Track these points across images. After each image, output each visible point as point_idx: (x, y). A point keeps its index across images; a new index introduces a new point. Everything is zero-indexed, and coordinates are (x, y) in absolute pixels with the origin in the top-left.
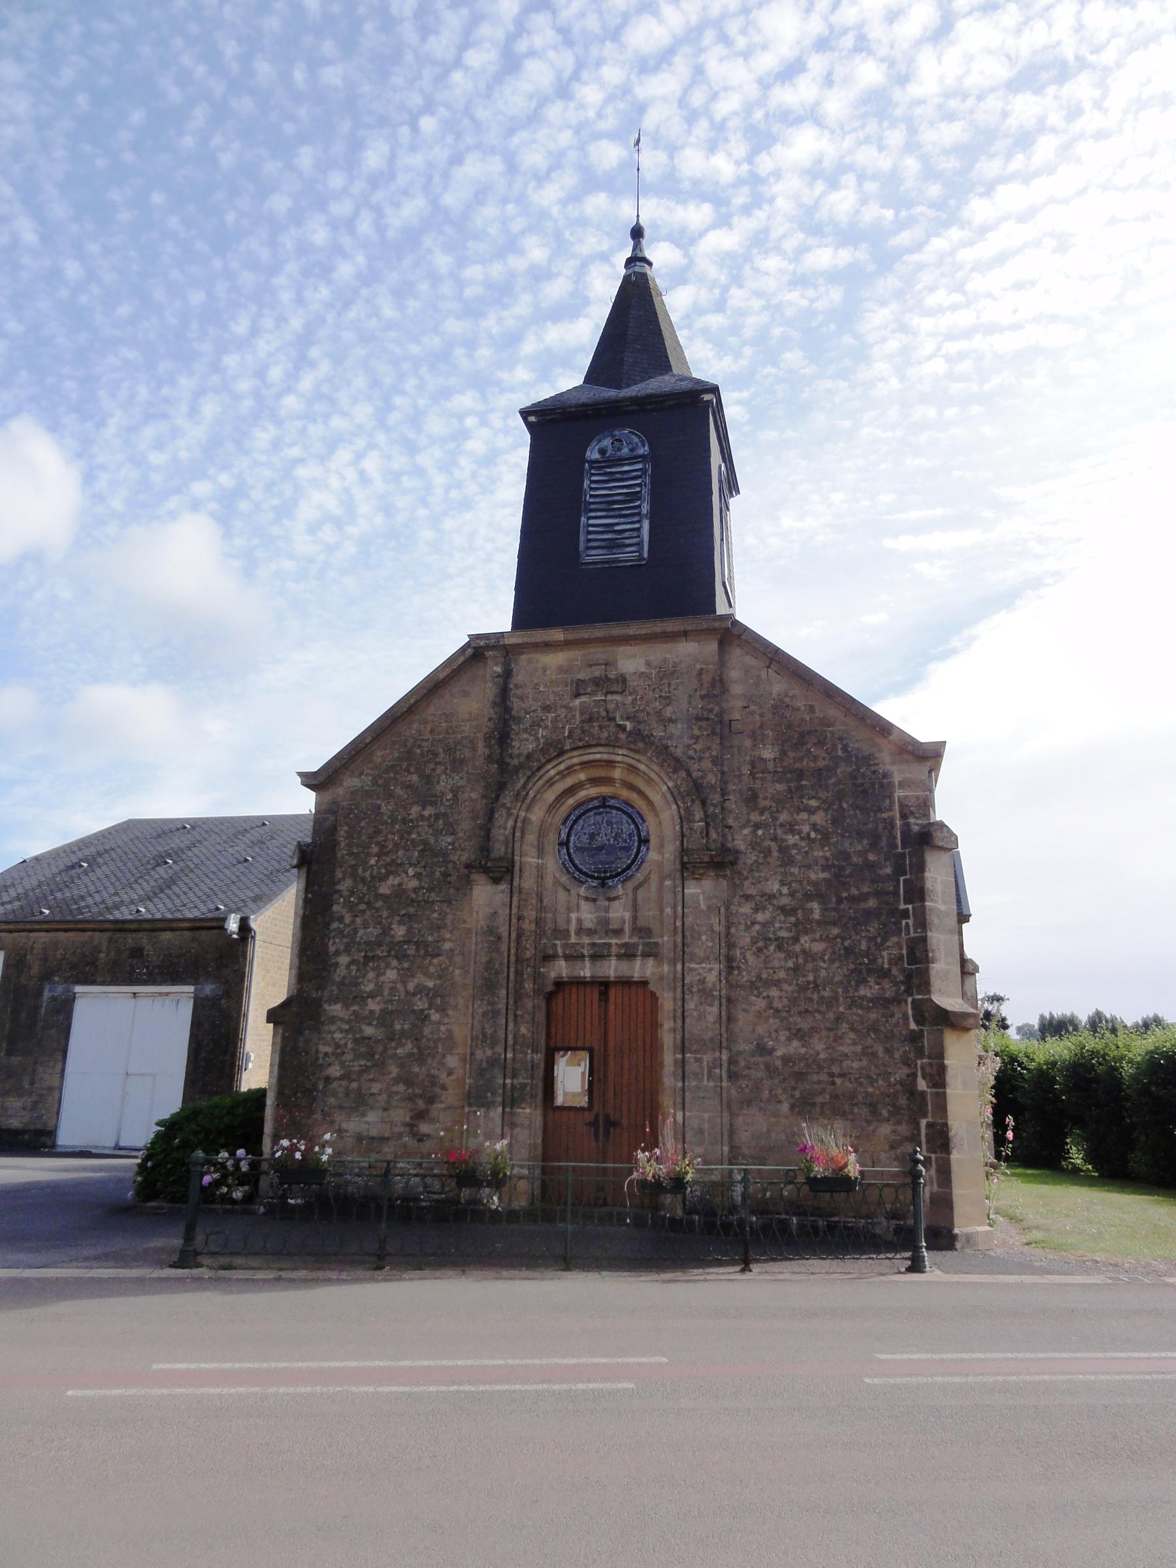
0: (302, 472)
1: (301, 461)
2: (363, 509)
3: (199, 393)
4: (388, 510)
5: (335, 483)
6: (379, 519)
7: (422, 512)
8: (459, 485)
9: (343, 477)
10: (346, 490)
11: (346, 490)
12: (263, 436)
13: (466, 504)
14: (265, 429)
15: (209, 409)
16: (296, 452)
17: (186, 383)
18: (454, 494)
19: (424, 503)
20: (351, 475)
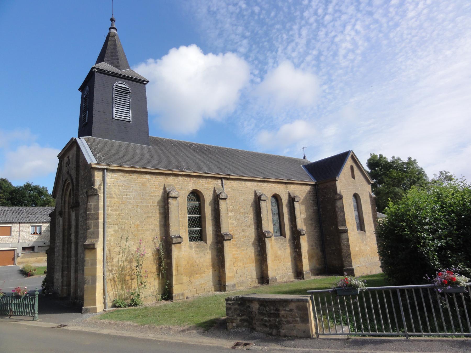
0: (337, 39)
1: (335, 36)
2: (360, 43)
3: (300, 28)
4: (368, 39)
5: (348, 38)
6: (366, 44)
7: (381, 35)
8: (392, 19)
9: (350, 35)
10: (353, 39)
11: (353, 39)
12: (322, 34)
13: (397, 25)
14: (322, 31)
15: (304, 32)
16: (333, 34)
17: (295, 27)
18: (391, 23)
19: (380, 31)
20: (353, 33)
